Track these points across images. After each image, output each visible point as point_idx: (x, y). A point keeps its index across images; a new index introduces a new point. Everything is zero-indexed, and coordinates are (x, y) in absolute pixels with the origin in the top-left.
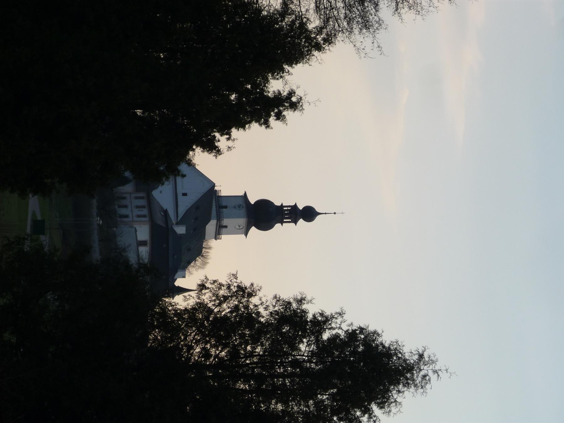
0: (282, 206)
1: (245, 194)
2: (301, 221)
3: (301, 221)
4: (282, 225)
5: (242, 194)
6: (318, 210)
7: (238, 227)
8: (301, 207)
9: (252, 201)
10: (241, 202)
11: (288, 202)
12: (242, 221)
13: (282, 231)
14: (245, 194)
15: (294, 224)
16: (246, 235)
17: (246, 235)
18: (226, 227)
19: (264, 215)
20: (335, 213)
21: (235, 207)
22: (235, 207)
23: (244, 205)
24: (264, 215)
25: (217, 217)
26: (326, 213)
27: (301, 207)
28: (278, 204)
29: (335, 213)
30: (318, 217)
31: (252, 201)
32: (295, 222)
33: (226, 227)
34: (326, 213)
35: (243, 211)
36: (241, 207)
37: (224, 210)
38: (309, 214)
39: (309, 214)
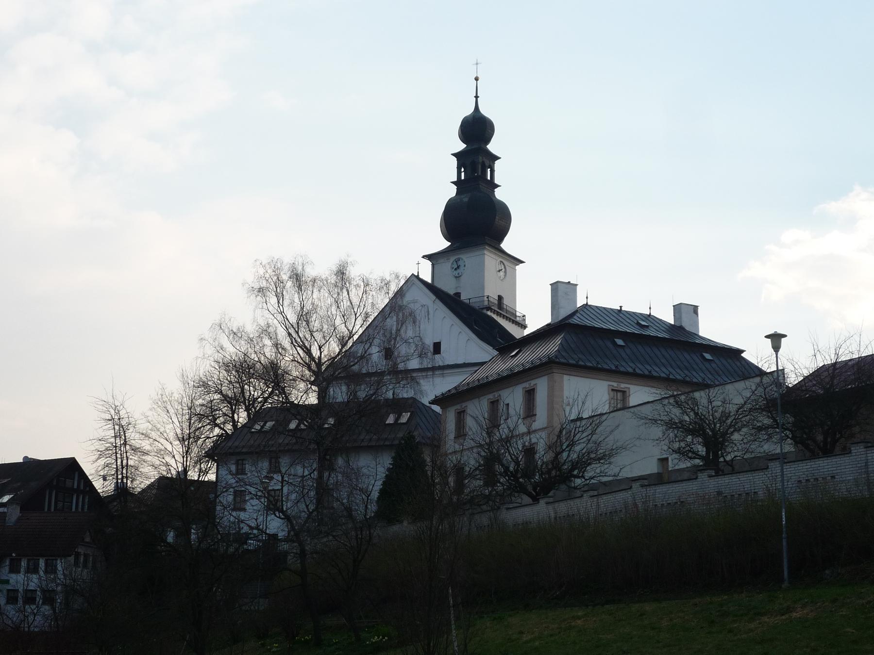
1: (429, 257)
2: (492, 147)
3: (492, 147)
4: (497, 186)
6: (469, 111)
7: (502, 274)
8: (461, 146)
10: (446, 266)
11: (450, 170)
12: (490, 260)
13: (509, 185)
14: (429, 257)
18: (500, 298)
19: (475, 218)
20: (477, 79)
21: (457, 277)
22: (457, 277)
23: (453, 259)
24: (475, 218)
26: (477, 97)
27: (461, 146)
28: (452, 191)
29: (477, 79)
30: (485, 111)
33: (500, 298)
34: (477, 97)
36: (460, 263)
38: (476, 130)
39: (476, 130)
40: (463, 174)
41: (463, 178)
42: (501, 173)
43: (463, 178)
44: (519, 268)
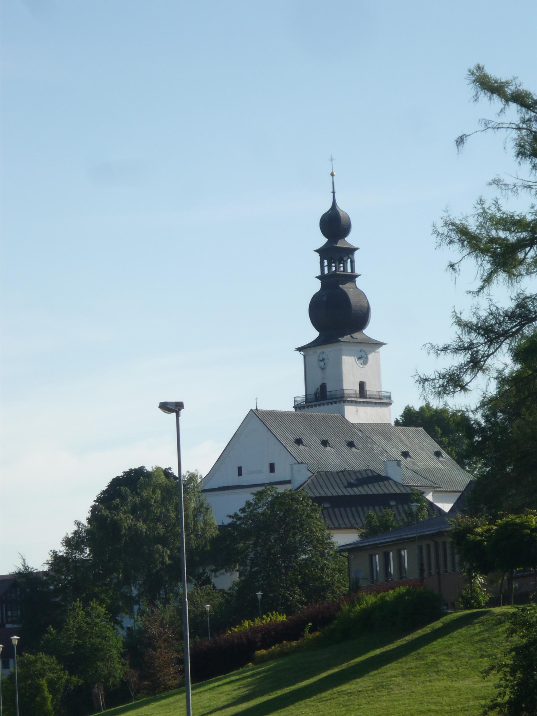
0: (322, 277)
1: (299, 349)
5: (300, 357)
6: (326, 207)
8: (322, 241)
9: (313, 334)
11: (313, 266)
14: (299, 349)
15: (356, 253)
16: (380, 344)
17: (380, 344)
18: (362, 385)
20: (332, 175)
21: (323, 369)
25: (340, 402)
26: (334, 192)
27: (322, 241)
28: (316, 286)
30: (342, 206)
31: (313, 334)
32: (351, 251)
33: (362, 385)
34: (334, 192)
35: (329, 350)
37: (328, 389)
38: (334, 225)
39: (334, 225)
40: (326, 269)
41: (326, 272)
42: (361, 263)
43: (326, 272)
44: (381, 349)
